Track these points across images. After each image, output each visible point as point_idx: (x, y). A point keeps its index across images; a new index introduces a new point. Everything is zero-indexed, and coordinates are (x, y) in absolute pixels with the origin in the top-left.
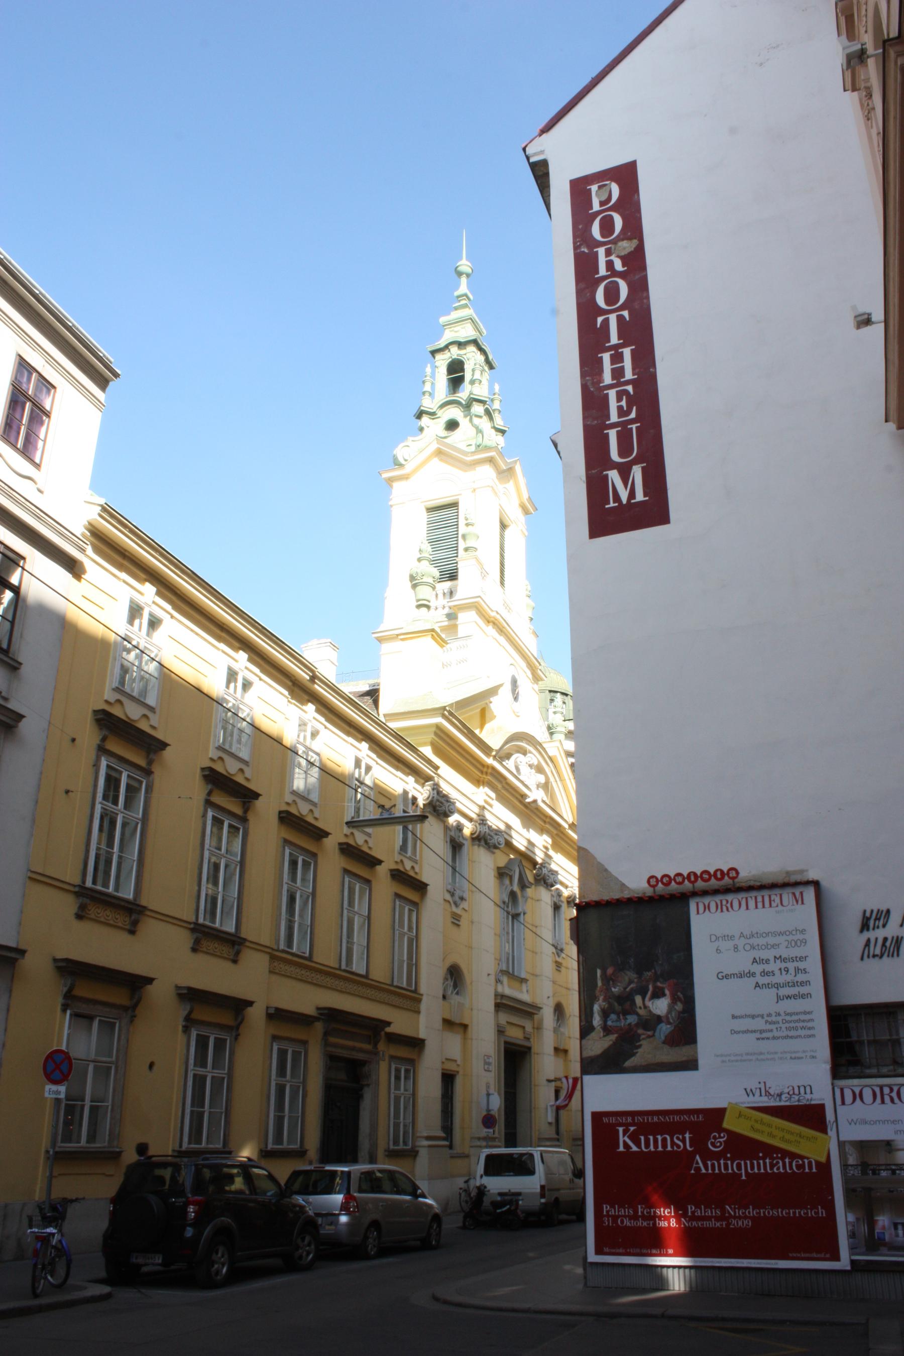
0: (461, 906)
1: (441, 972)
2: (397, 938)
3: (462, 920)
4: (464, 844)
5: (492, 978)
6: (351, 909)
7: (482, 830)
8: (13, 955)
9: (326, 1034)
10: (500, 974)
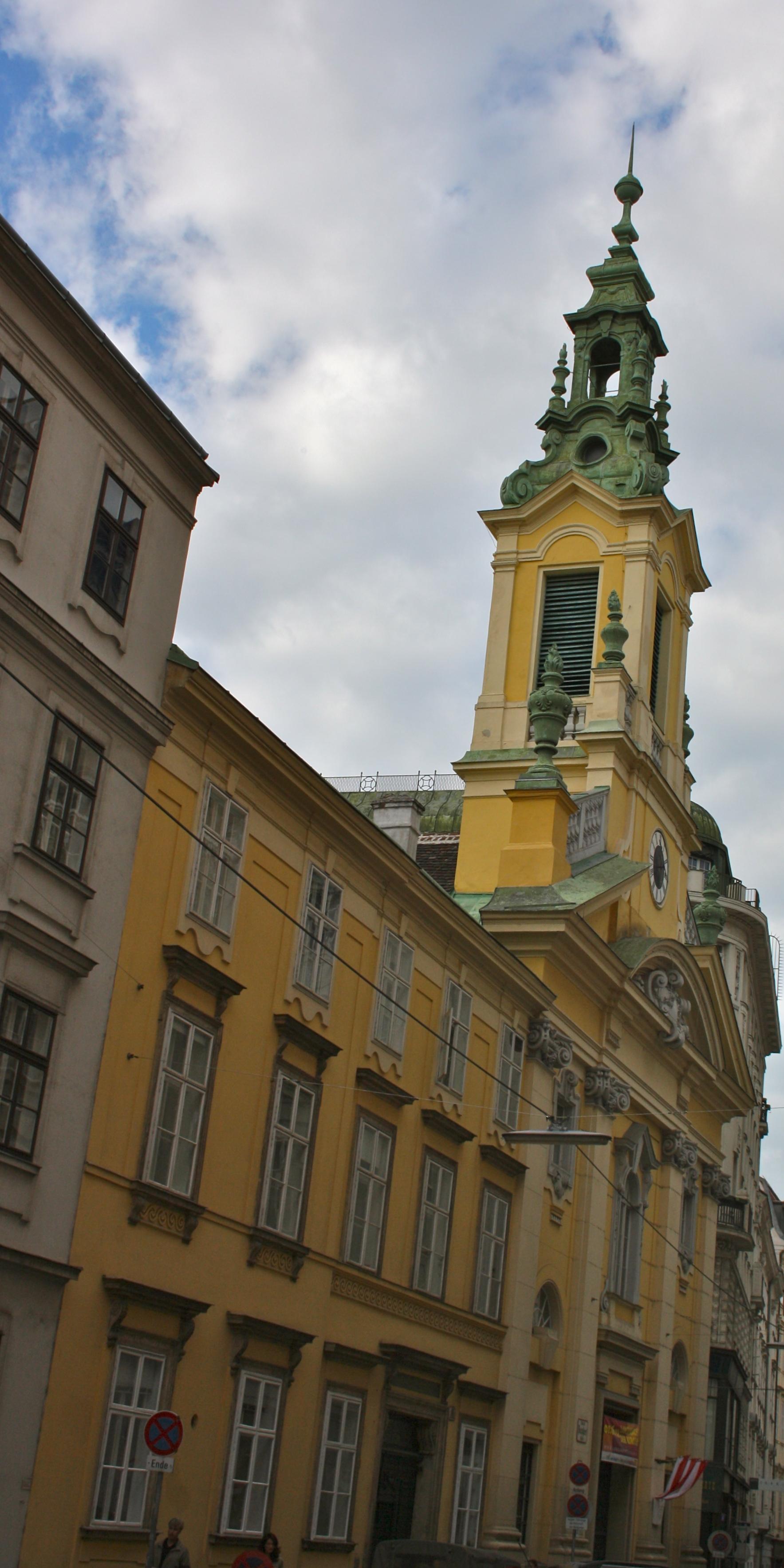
0: (564, 1198)
1: (533, 1295)
2: (482, 1244)
3: (564, 1217)
4: (574, 1105)
5: (597, 1303)
6: (431, 1204)
7: (601, 1085)
8: (65, 1274)
9: (388, 1381)
10: (606, 1299)
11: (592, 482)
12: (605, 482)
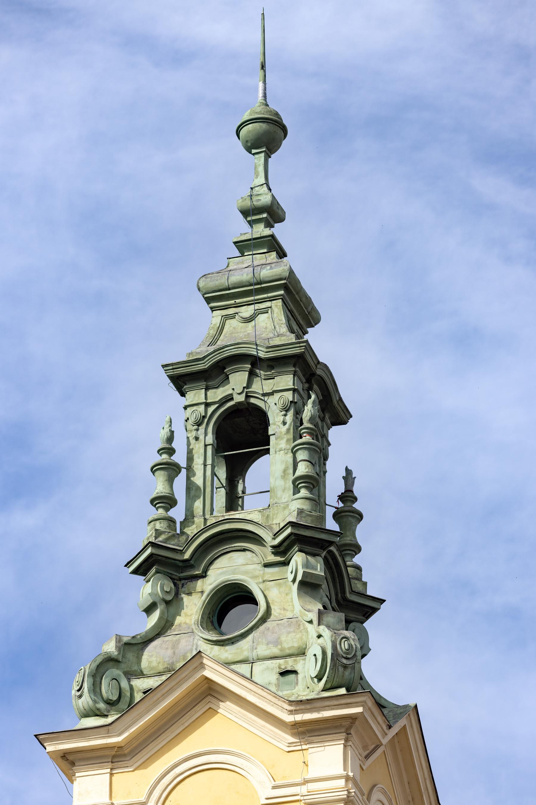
11: (233, 671)
12: (258, 667)
